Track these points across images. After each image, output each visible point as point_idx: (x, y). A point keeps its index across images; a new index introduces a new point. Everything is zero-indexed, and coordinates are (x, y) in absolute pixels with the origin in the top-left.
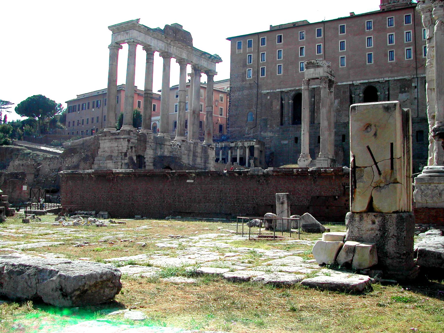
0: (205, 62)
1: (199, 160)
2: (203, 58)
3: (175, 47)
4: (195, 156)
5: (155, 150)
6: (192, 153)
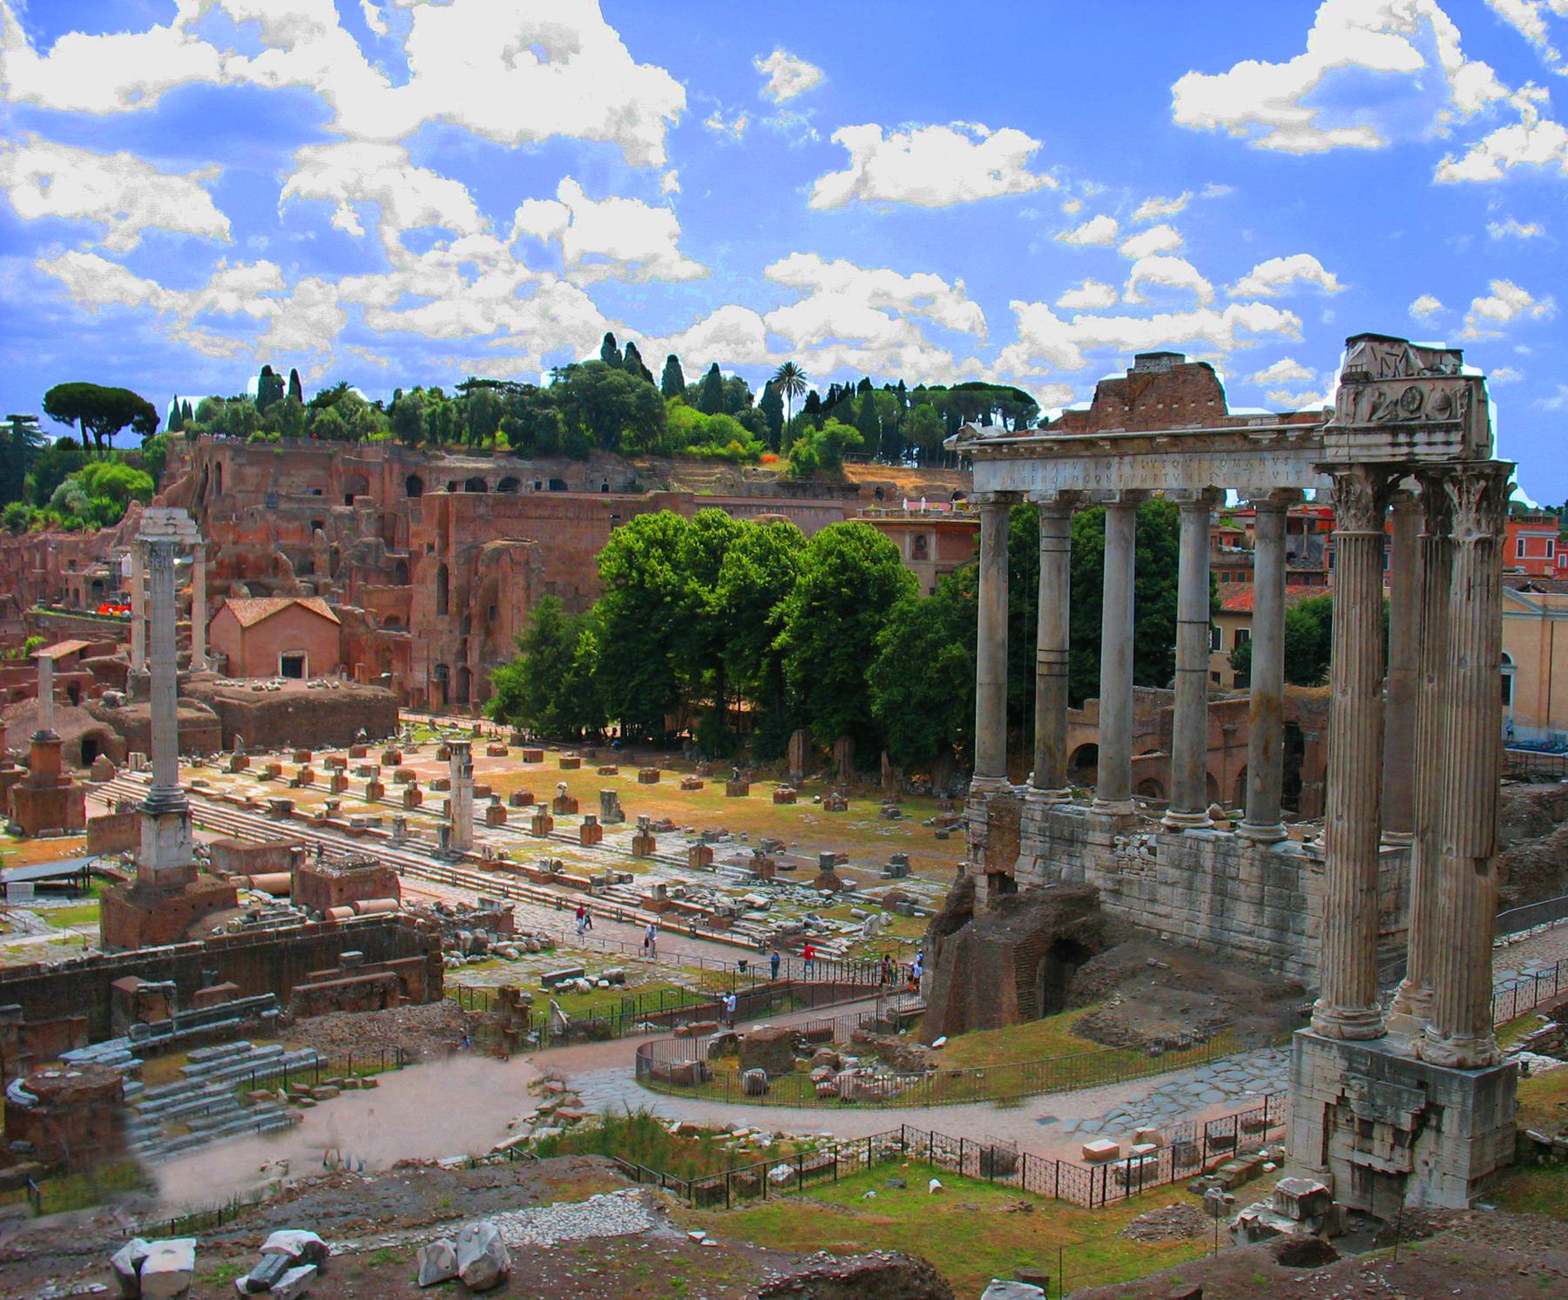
0: (1281, 467)
1: (1243, 914)
2: (1270, 449)
3: (1127, 459)
4: (1223, 894)
5: (1047, 857)
6: (1209, 879)
